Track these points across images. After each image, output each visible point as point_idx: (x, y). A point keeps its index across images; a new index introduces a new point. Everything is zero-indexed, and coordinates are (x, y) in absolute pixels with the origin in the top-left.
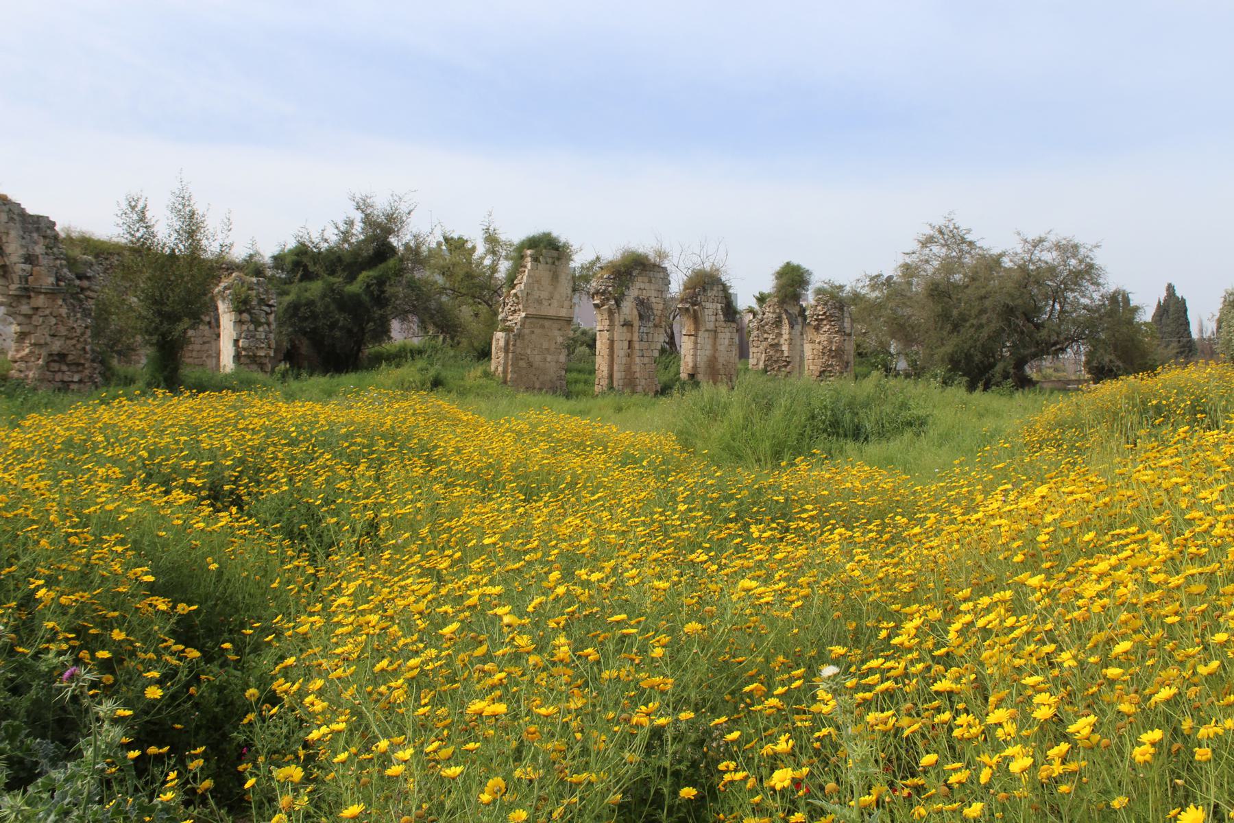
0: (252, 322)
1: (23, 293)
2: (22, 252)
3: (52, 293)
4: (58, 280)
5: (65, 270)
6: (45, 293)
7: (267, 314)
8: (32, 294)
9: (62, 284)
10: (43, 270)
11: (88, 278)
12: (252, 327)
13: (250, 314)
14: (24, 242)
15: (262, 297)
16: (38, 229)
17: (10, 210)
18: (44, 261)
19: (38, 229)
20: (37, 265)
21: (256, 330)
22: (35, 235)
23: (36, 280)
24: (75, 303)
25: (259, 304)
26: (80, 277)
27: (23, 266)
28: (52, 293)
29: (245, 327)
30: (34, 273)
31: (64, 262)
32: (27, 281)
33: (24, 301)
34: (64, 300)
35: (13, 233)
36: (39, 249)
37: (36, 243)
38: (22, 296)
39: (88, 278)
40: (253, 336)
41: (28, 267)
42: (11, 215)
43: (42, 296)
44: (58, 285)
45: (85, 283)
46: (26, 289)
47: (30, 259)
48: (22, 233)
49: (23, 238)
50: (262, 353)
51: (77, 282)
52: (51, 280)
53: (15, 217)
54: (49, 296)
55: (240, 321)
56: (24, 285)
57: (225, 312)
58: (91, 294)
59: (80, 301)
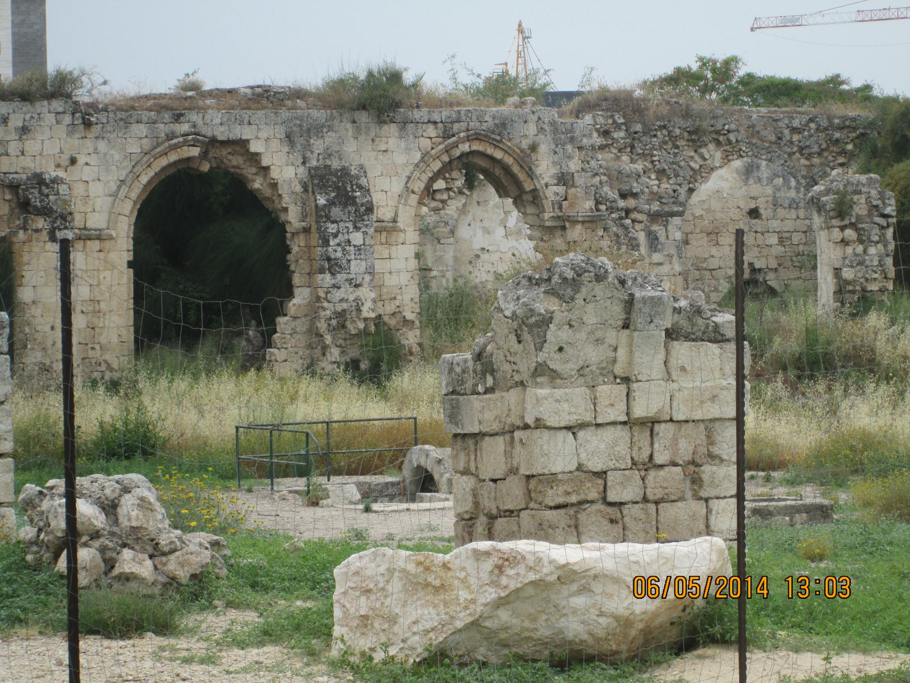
0: (861, 241)
1: (557, 224)
2: (554, 171)
3: (591, 222)
4: (598, 203)
5: (606, 189)
6: (583, 222)
7: (882, 228)
8: (567, 224)
9: (603, 207)
10: (580, 192)
11: (635, 195)
12: (860, 249)
13: (857, 230)
14: (556, 158)
15: (875, 203)
16: (572, 139)
17: (539, 118)
18: (580, 180)
19: (572, 139)
20: (573, 186)
21: (865, 251)
22: (569, 147)
23: (571, 205)
24: (620, 232)
25: (870, 214)
26: (623, 196)
27: (555, 188)
28: (591, 222)
29: (849, 250)
30: (569, 197)
31: (604, 178)
32: (560, 208)
33: (558, 233)
34: (605, 229)
35: (543, 148)
36: (574, 165)
37: (570, 157)
38: (556, 227)
39: (635, 195)
40: (861, 263)
41: (561, 189)
42: (541, 124)
43: (579, 227)
44: (598, 210)
45: (631, 203)
46: (559, 217)
47: (564, 179)
48: (553, 146)
49: (556, 153)
50: (874, 287)
51: (621, 204)
52: (590, 204)
53: (546, 127)
54: (587, 225)
55: (843, 241)
56: (558, 213)
57: (821, 228)
58: (640, 217)
59: (626, 228)
